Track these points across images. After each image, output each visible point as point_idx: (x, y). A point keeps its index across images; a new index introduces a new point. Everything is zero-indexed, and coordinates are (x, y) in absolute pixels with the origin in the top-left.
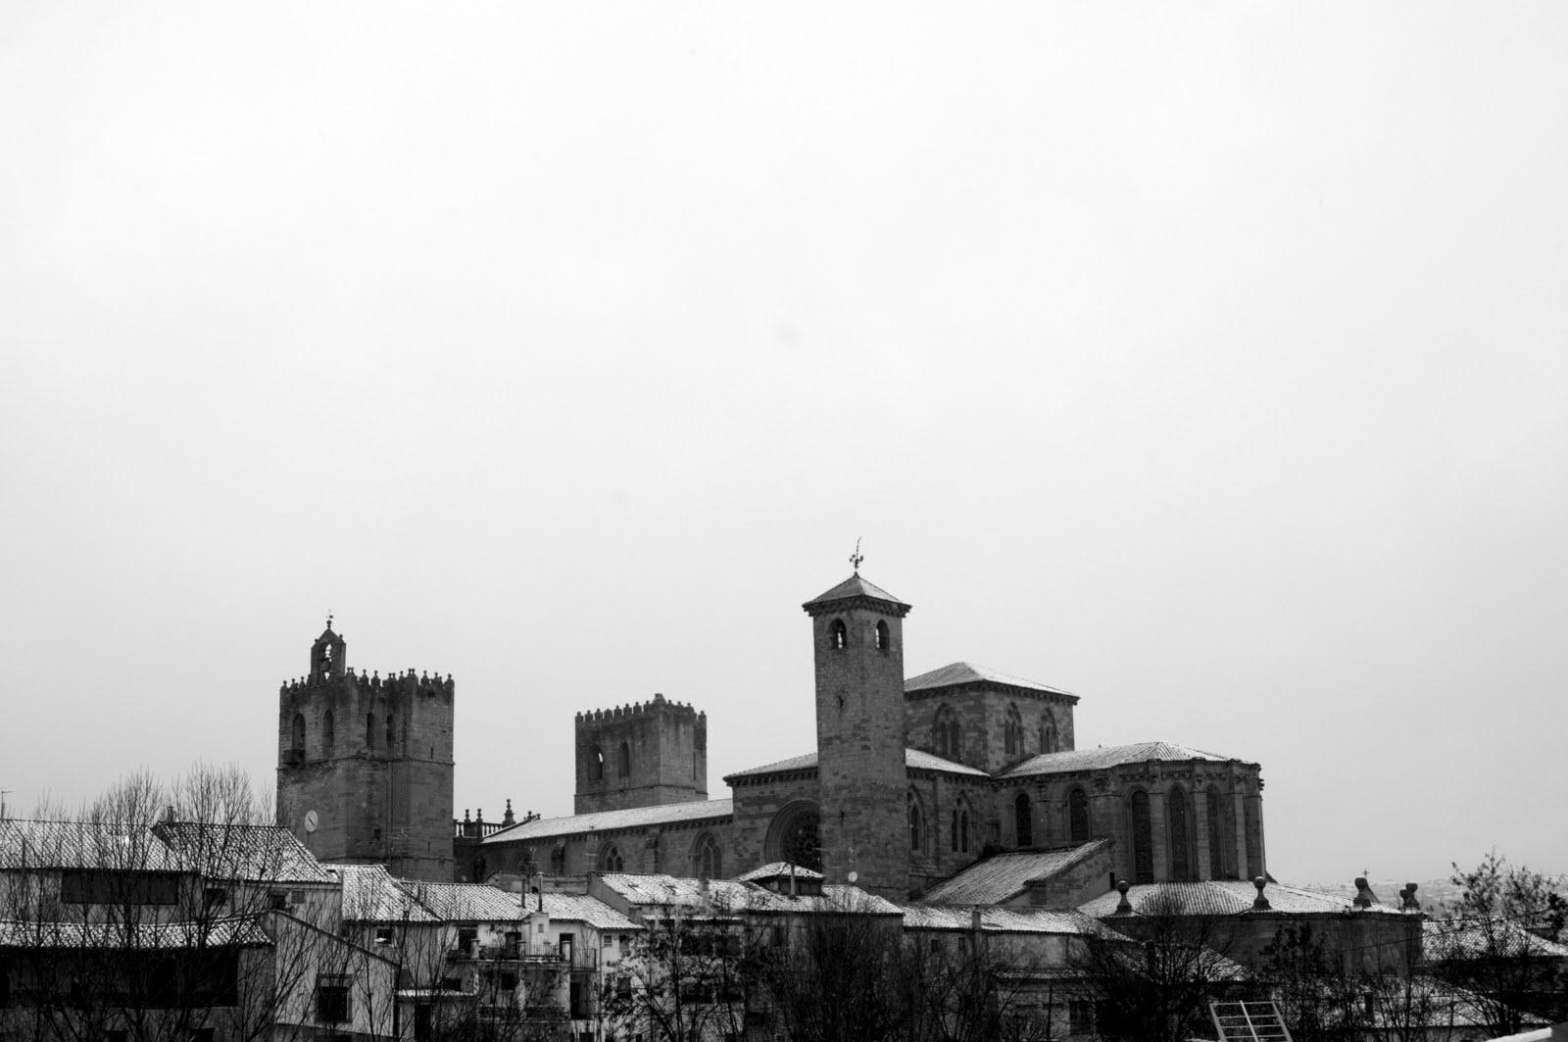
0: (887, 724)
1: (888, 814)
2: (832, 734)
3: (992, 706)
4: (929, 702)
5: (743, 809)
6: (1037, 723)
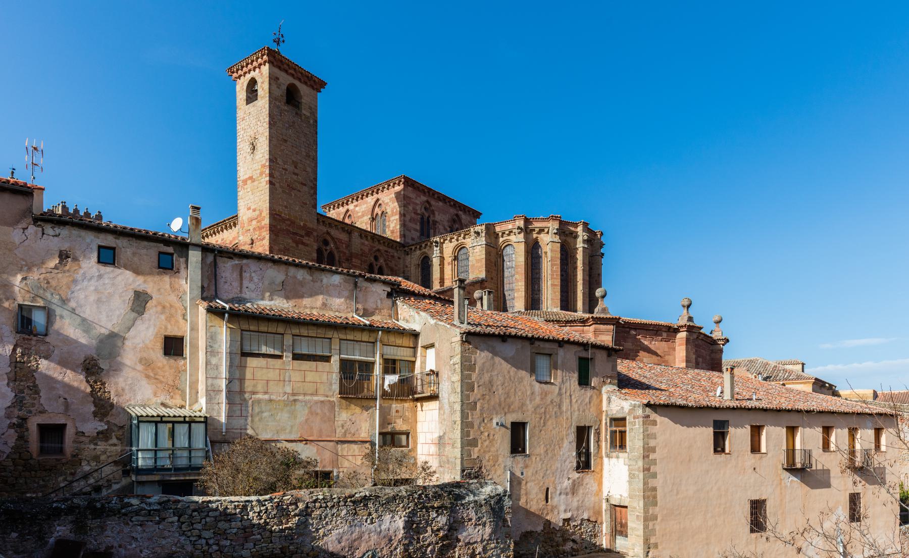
0: (296, 171)
1: (294, 245)
2: (246, 177)
3: (410, 198)
6: (448, 221)
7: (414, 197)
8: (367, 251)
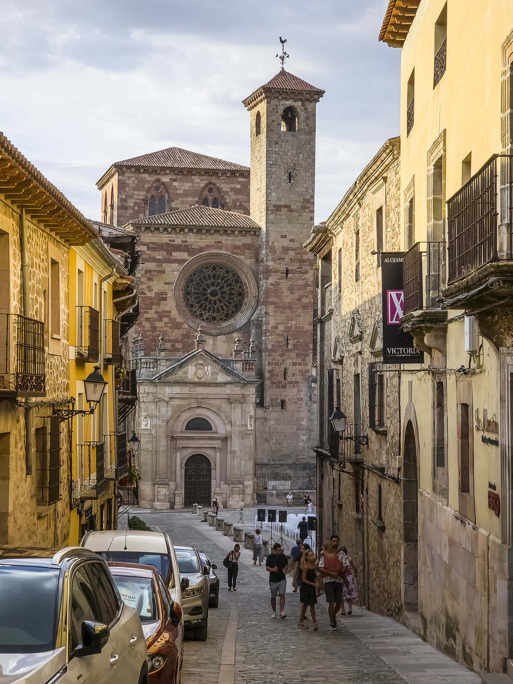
2: (282, 203)
4: (196, 179)
5: (149, 252)
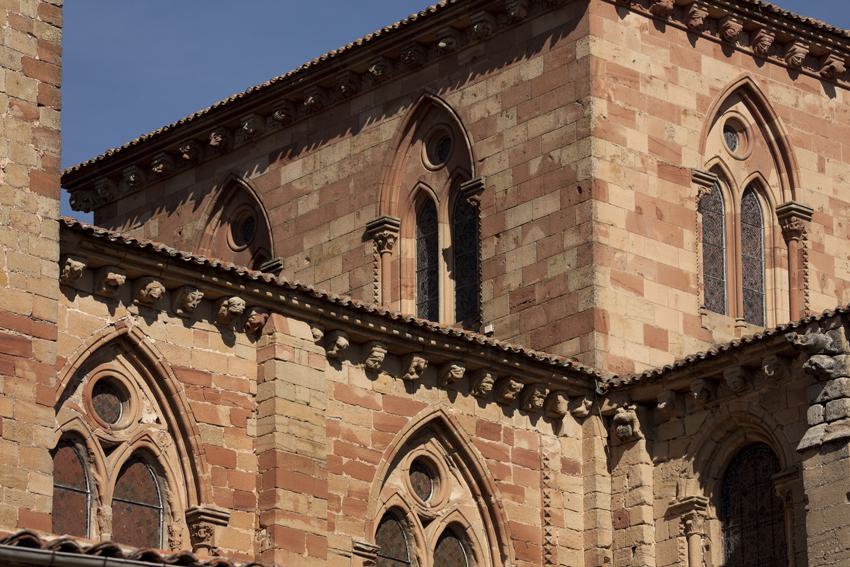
3: (632, 78)
7: (658, 71)
8: (365, 434)
